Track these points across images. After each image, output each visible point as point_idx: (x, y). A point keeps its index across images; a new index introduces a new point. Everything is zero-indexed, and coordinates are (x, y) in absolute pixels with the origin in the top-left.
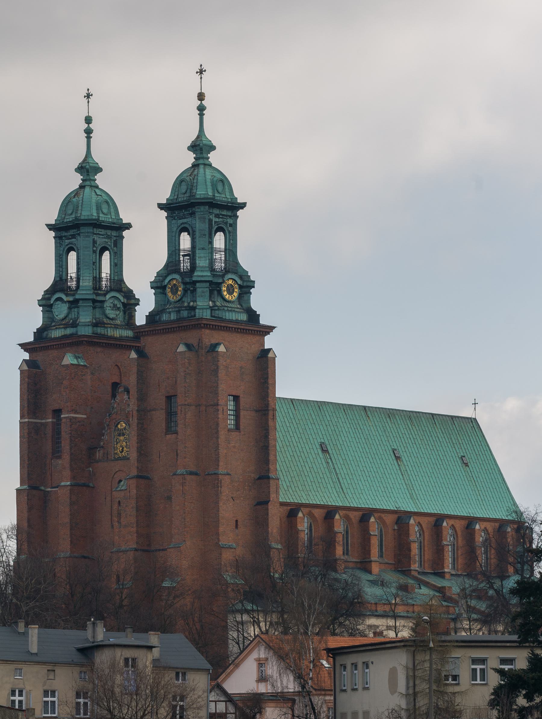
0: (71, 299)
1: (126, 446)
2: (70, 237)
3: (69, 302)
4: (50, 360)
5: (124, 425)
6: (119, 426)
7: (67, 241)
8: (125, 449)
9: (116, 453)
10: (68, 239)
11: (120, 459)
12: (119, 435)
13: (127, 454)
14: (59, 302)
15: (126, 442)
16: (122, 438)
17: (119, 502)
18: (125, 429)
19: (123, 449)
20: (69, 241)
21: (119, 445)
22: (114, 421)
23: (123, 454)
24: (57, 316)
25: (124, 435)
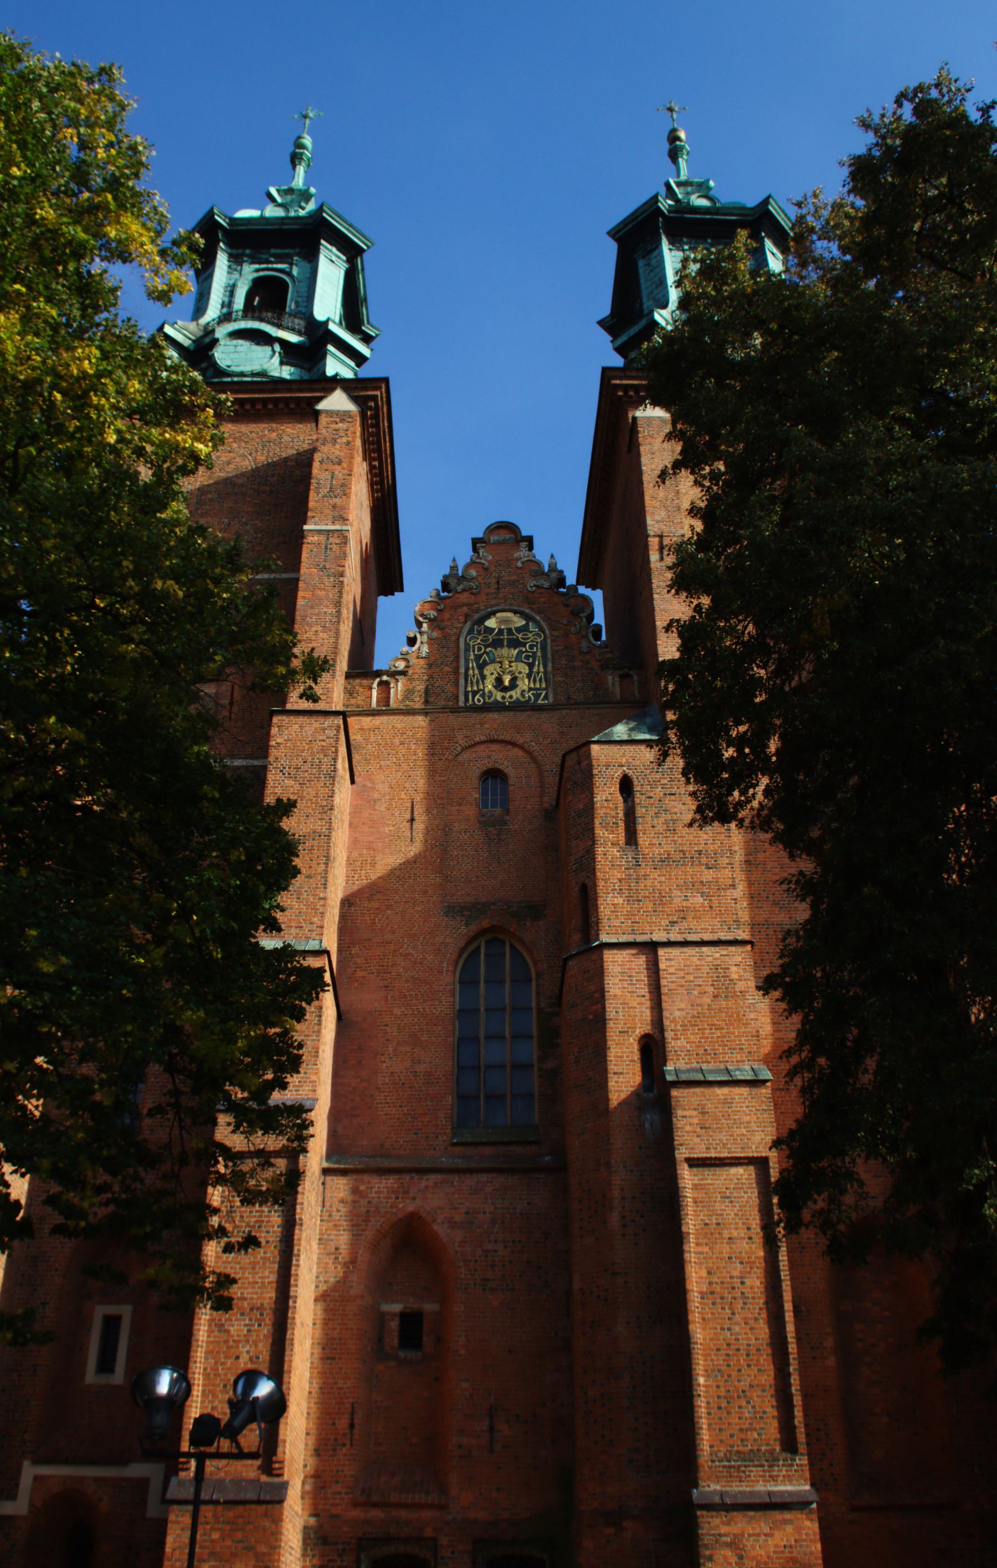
0: (293, 338)
3: (283, 343)
5: (519, 622)
6: (491, 623)
7: (257, 266)
8: (524, 684)
9: (475, 693)
10: (260, 263)
11: (499, 707)
12: (497, 644)
13: (537, 696)
14: (240, 342)
15: (531, 666)
19: (514, 680)
22: (465, 609)
23: (515, 694)
24: (229, 367)
25: (514, 643)
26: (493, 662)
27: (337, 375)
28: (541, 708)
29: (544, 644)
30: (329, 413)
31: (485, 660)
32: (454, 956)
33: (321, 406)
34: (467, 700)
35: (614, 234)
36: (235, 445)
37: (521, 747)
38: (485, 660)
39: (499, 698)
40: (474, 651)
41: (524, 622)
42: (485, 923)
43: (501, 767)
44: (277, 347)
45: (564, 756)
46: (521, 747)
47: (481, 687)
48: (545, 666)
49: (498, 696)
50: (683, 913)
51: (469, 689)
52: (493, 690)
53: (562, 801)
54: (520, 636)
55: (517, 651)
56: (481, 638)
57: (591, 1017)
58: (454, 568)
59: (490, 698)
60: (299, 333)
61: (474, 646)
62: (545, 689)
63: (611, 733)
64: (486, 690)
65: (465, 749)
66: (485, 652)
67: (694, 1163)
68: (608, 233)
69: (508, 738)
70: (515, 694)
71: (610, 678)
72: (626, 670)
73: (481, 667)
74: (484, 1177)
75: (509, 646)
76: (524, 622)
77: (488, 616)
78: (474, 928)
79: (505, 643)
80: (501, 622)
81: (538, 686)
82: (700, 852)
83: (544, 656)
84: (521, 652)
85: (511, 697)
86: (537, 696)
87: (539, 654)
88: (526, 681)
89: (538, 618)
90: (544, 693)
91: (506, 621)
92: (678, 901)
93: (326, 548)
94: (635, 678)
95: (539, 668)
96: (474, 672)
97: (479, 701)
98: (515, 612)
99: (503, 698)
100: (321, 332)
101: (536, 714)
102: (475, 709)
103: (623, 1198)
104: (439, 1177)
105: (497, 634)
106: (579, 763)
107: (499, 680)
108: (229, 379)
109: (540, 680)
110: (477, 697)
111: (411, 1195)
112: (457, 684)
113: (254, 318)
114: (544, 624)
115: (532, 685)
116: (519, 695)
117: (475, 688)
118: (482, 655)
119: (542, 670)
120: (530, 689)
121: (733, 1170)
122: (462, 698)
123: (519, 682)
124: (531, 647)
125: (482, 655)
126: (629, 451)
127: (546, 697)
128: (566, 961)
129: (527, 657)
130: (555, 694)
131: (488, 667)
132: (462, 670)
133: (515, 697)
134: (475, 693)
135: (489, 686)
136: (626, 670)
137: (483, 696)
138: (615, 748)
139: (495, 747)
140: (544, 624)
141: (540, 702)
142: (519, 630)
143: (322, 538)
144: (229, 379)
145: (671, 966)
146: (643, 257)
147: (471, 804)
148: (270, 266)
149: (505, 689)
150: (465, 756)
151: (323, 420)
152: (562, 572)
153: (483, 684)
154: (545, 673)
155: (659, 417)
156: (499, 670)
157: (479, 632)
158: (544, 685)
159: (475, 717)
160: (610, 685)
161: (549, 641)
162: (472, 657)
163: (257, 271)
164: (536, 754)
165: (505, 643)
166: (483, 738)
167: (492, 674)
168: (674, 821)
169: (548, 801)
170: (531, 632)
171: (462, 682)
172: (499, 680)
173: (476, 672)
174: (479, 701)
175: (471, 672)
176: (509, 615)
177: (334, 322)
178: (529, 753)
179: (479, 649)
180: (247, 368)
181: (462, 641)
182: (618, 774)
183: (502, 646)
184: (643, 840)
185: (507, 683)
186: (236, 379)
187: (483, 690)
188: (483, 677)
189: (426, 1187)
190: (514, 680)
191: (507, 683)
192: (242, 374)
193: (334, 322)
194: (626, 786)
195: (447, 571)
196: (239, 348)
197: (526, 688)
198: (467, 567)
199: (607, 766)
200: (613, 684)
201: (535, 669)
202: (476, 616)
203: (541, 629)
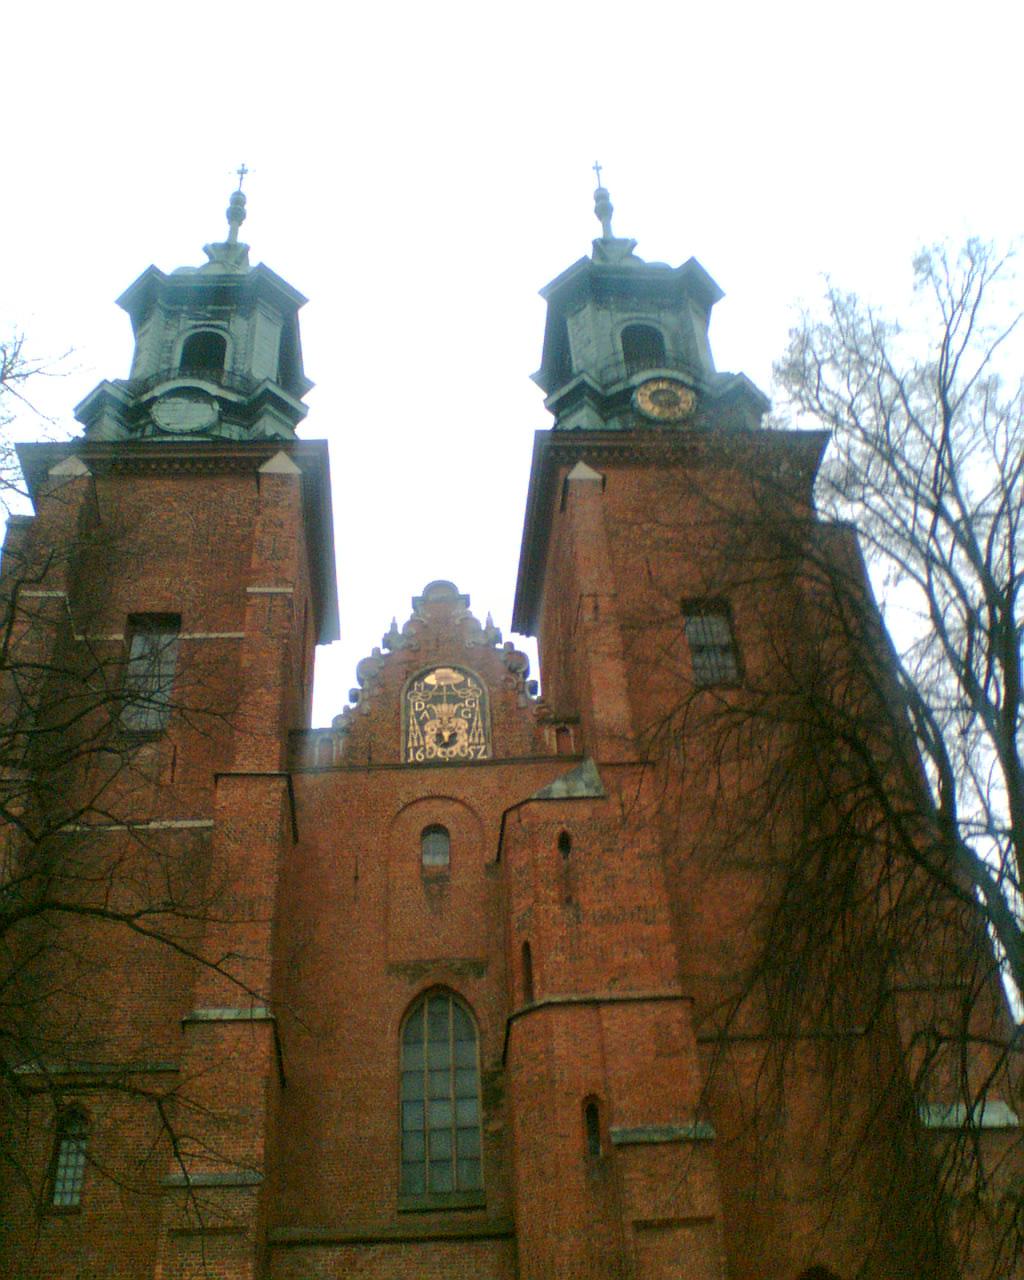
1: (468, 731)
2: (209, 315)
4: (141, 500)
5: (457, 677)
6: (431, 680)
7: (194, 322)
8: (462, 739)
10: (197, 319)
12: (437, 700)
13: (476, 752)
14: (180, 400)
15: (470, 721)
16: (443, 708)
17: (565, 842)
18: (461, 685)
19: (453, 736)
20: (202, 322)
21: (431, 728)
23: (455, 749)
25: (453, 700)
26: (433, 717)
27: (277, 434)
28: (482, 763)
29: (482, 699)
30: (270, 475)
31: (425, 718)
32: (398, 1017)
33: (264, 469)
34: (408, 756)
35: (542, 293)
36: (175, 504)
37: (462, 802)
38: (425, 718)
39: (440, 755)
40: (414, 707)
41: (462, 678)
42: (428, 983)
43: (442, 823)
44: (216, 406)
45: (505, 814)
46: (462, 802)
47: (422, 743)
48: (484, 720)
49: (439, 752)
50: (624, 970)
51: (410, 745)
52: (434, 746)
53: (502, 856)
54: (459, 692)
55: (456, 707)
56: (420, 694)
57: (536, 1078)
58: (394, 625)
59: (430, 754)
60: (239, 392)
61: (414, 704)
62: (485, 744)
63: (550, 791)
64: (427, 747)
65: (406, 806)
66: (425, 708)
67: (643, 1226)
68: (540, 293)
69: (449, 794)
70: (455, 749)
71: (546, 732)
72: (562, 725)
73: (422, 724)
74: (431, 1246)
75: (448, 703)
76: (462, 678)
77: (428, 672)
78: (417, 988)
79: (445, 699)
80: (439, 679)
81: (477, 740)
82: (639, 908)
83: (483, 713)
84: (460, 708)
85: (451, 753)
86: (476, 752)
87: (477, 709)
88: (466, 736)
89: (476, 674)
90: (483, 748)
91: (447, 678)
92: (618, 958)
93: (270, 611)
94: (571, 732)
95: (478, 722)
96: (414, 728)
97: (420, 757)
98: (454, 669)
99: (444, 753)
100: (259, 391)
101: (477, 770)
102: (417, 765)
103: (572, 1264)
104: (387, 1247)
105: (436, 691)
106: (520, 821)
107: (439, 736)
108: (169, 439)
109: (480, 735)
110: (419, 753)
111: (358, 1266)
112: (398, 742)
113: (192, 376)
114: (482, 681)
115: (471, 740)
116: (459, 750)
117: (416, 744)
118: (422, 712)
119: (480, 724)
120: (469, 745)
121: (679, 1232)
122: (403, 754)
123: (459, 738)
124: (470, 703)
125: (422, 712)
126: (563, 508)
127: (485, 753)
128: (509, 1023)
129: (466, 713)
130: (494, 747)
131: (429, 724)
132: (403, 727)
133: (455, 753)
134: (416, 749)
135: (430, 741)
136: (562, 725)
137: (424, 752)
138: (554, 808)
139: (437, 803)
140: (482, 681)
141: (480, 757)
142: (458, 686)
143: (267, 600)
144: (169, 439)
145: (614, 1025)
146: (573, 315)
147: (414, 861)
148: (207, 323)
149: (446, 745)
150: (406, 814)
151: (265, 482)
152: (498, 629)
153: (424, 740)
154: (484, 728)
155: (589, 480)
156: (439, 726)
157: (419, 689)
158: (482, 740)
159: (416, 774)
160: (547, 739)
161: (487, 698)
162: (412, 713)
163: (195, 327)
164: (476, 809)
165: (445, 699)
166: (425, 794)
167: (433, 730)
168: (613, 877)
169: (490, 855)
170: (469, 688)
171: (403, 738)
172: (439, 736)
173: (417, 727)
174: (420, 757)
175: (411, 728)
176: (449, 671)
177: (271, 381)
178: (470, 808)
179: (420, 706)
180: (187, 426)
181: (402, 697)
182: (557, 830)
183: (441, 703)
184: (582, 897)
185: (446, 739)
186: (176, 439)
187: (424, 746)
188: (424, 733)
189: (374, 1258)
190: (453, 736)
191: (446, 739)
192: (183, 433)
193: (271, 381)
194: (565, 842)
195: (388, 630)
196: (178, 406)
197: (466, 744)
198: (408, 625)
199: (547, 823)
200: (550, 739)
201: (474, 724)
202: (416, 673)
203: (480, 686)
